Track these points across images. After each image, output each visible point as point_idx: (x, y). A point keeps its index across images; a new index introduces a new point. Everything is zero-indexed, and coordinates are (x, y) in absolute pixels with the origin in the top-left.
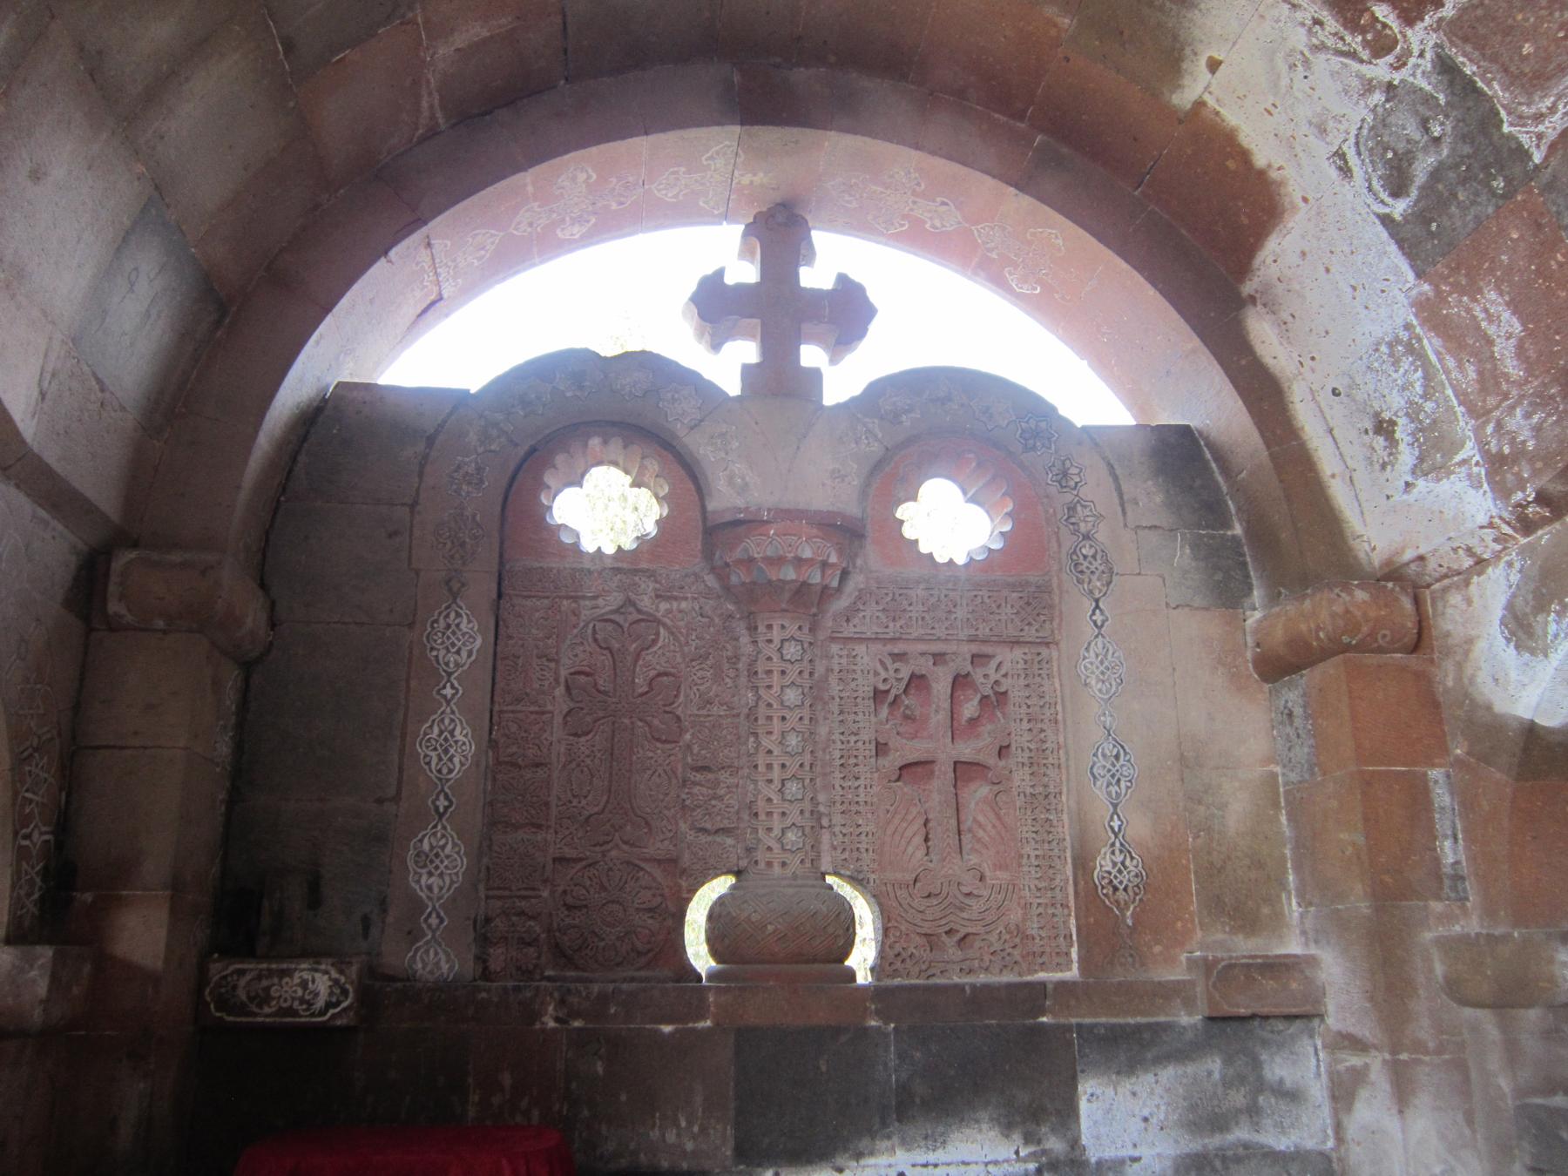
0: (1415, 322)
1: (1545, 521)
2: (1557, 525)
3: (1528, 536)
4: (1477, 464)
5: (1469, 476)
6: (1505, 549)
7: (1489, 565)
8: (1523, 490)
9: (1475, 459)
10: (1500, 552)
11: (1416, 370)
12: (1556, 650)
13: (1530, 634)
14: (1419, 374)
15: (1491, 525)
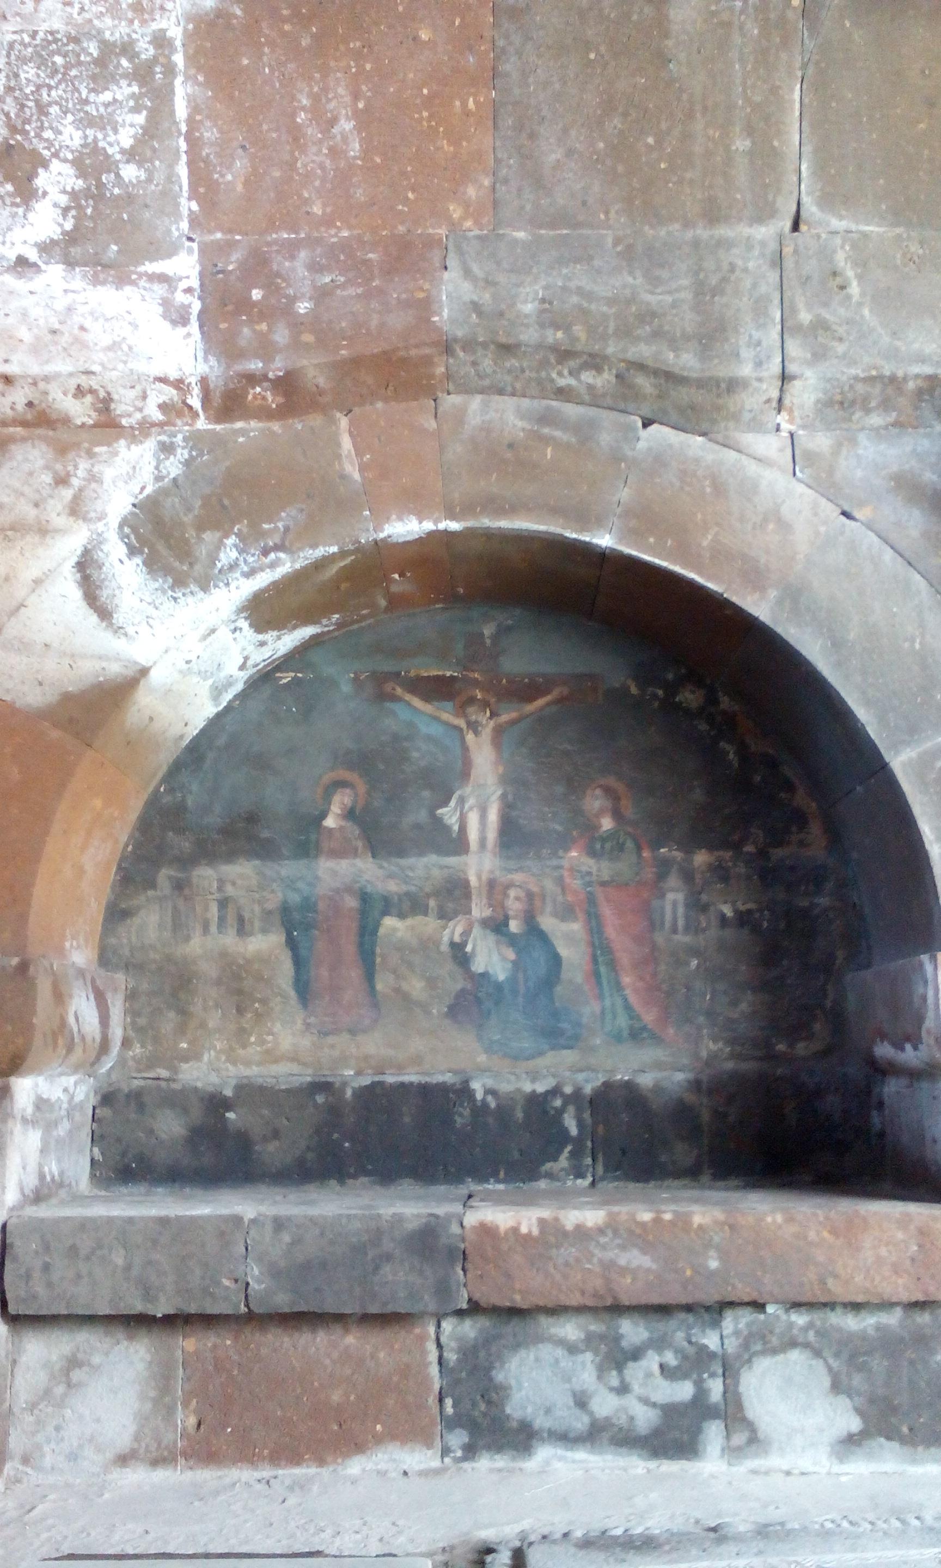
0: (178, 43)
1: (265, 414)
2: (276, 427)
3: (218, 420)
4: (189, 290)
5: (166, 303)
6: (161, 425)
7: (117, 439)
8: (267, 359)
9: (183, 285)
10: (153, 425)
11: (136, 110)
12: (227, 584)
13: (184, 552)
14: (140, 119)
15: (179, 384)
